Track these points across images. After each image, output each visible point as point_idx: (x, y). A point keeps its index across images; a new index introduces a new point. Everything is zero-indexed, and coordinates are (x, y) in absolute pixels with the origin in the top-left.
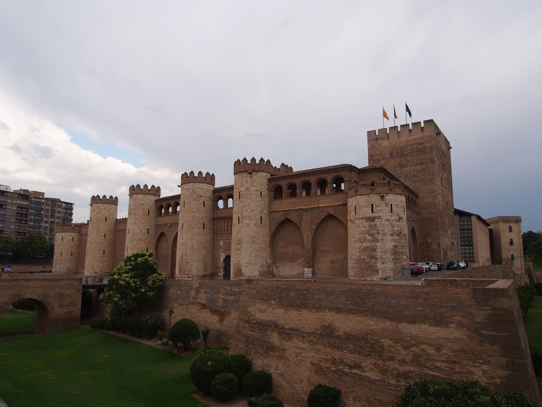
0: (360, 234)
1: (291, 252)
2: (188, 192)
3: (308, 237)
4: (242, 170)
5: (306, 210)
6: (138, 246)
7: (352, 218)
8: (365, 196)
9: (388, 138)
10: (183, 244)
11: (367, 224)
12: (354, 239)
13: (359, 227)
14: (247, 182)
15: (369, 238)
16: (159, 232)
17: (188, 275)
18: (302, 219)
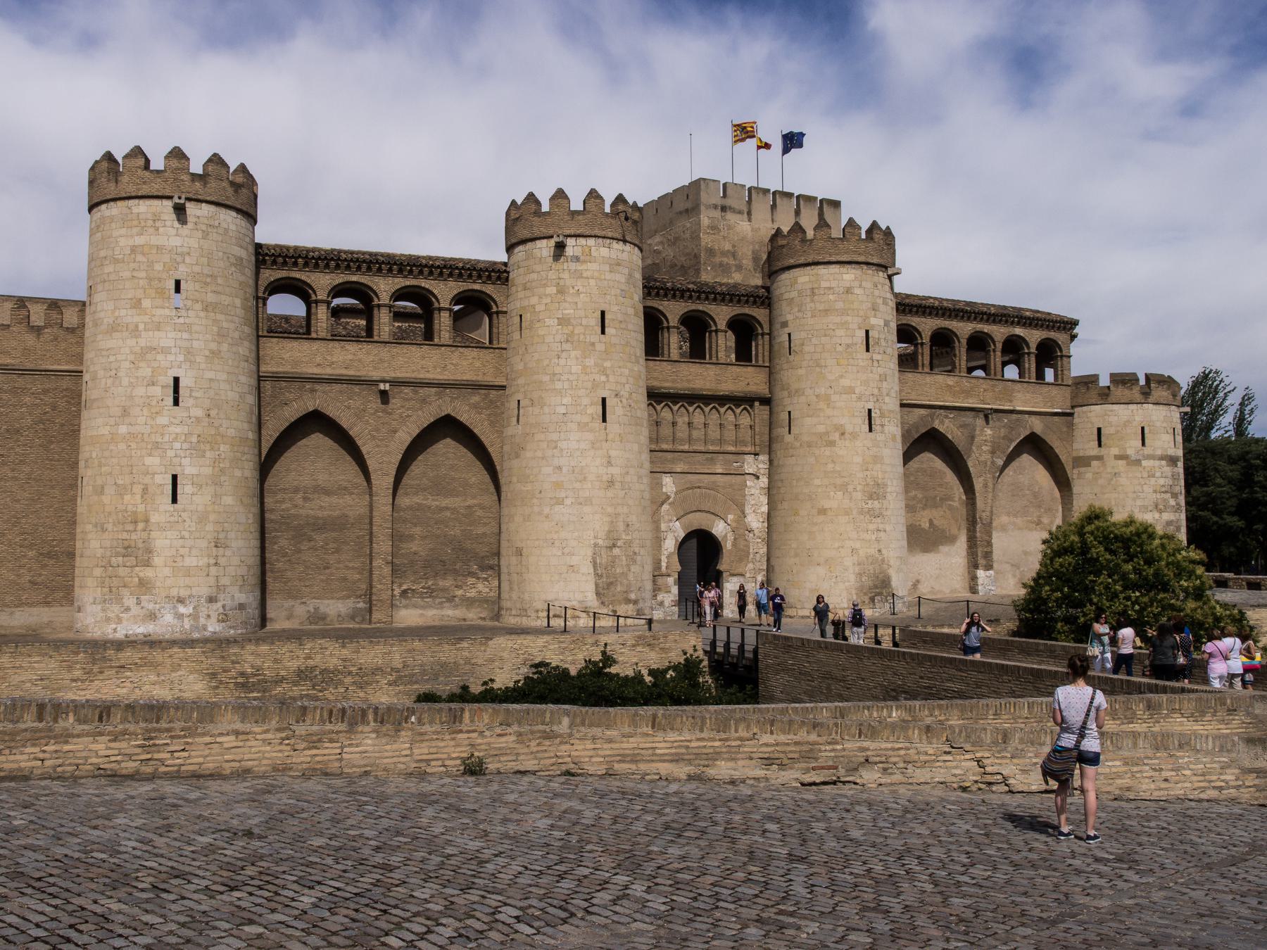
0: (1155, 492)
1: (926, 525)
2: (618, 277)
3: (986, 486)
4: (875, 261)
5: (987, 415)
6: (238, 473)
7: (1130, 452)
8: (1165, 408)
9: (749, 213)
10: (611, 483)
11: (1168, 470)
12: (1139, 503)
13: (1153, 476)
14: (885, 303)
15: (1172, 502)
16: (291, 413)
17: (635, 602)
18: (973, 438)
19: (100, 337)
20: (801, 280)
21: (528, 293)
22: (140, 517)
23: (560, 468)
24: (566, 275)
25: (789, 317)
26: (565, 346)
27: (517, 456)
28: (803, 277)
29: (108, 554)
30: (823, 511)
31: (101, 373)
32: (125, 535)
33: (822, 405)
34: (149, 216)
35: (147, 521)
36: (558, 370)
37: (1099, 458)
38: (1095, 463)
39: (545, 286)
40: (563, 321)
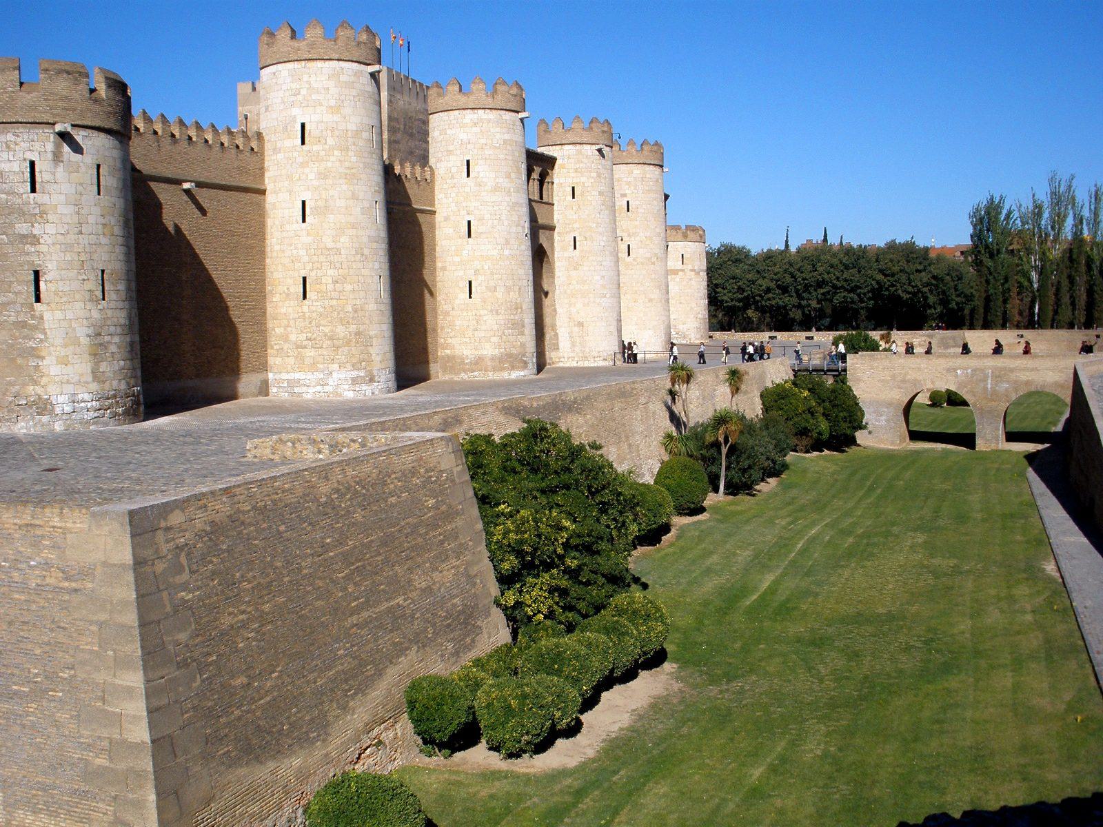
7: (696, 268)
19: (483, 194)
20: (635, 172)
21: (579, 174)
22: (519, 306)
23: (603, 277)
24: (600, 167)
25: (627, 192)
26: (603, 207)
27: (576, 269)
28: (637, 170)
29: (502, 328)
30: (651, 300)
31: (487, 217)
32: (512, 317)
33: (648, 242)
34: (511, 122)
35: (521, 308)
36: (599, 221)
37: (683, 270)
38: (680, 273)
39: (590, 172)
40: (601, 193)
